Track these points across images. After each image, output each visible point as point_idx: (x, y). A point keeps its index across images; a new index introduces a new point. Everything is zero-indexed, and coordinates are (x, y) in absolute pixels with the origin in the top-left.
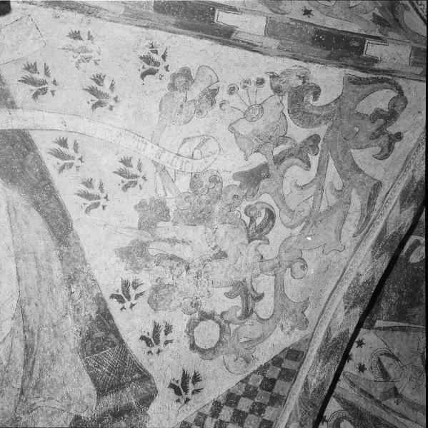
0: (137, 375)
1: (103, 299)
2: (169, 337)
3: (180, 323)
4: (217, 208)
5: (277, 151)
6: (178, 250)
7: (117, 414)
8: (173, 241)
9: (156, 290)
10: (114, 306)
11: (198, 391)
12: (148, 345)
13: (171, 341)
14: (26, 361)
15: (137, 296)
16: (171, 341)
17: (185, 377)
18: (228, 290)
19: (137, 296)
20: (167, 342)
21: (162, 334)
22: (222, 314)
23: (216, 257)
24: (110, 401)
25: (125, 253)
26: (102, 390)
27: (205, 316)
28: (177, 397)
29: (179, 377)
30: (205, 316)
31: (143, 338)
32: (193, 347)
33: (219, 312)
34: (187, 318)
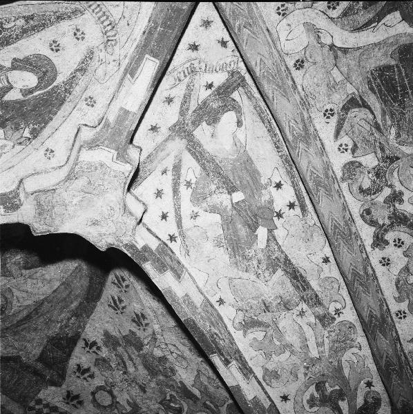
0: (60, 372)
1: (79, 337)
2: (89, 379)
3: (98, 382)
4: (161, 378)
5: (208, 403)
6: (129, 363)
7: (36, 373)
8: (131, 359)
9: (104, 360)
10: (81, 344)
11: (76, 407)
12: (78, 370)
13: (87, 381)
14: (21, 321)
15: (94, 352)
16: (87, 381)
17: (77, 397)
18: (131, 401)
19: (94, 352)
20: (85, 379)
21: (88, 374)
22: (118, 402)
23: (140, 386)
24: (39, 366)
25: (107, 334)
26: (42, 358)
27: (110, 393)
28: (65, 398)
29: (75, 393)
30: (110, 393)
31: (78, 365)
32: (93, 394)
33: (118, 400)
34: (103, 384)
